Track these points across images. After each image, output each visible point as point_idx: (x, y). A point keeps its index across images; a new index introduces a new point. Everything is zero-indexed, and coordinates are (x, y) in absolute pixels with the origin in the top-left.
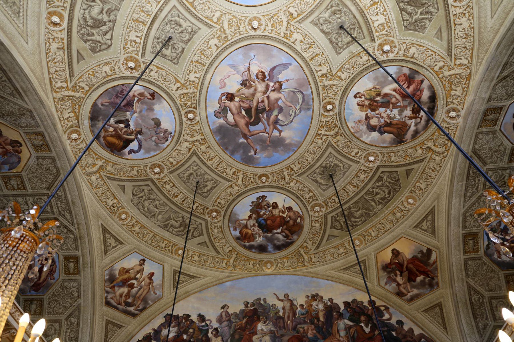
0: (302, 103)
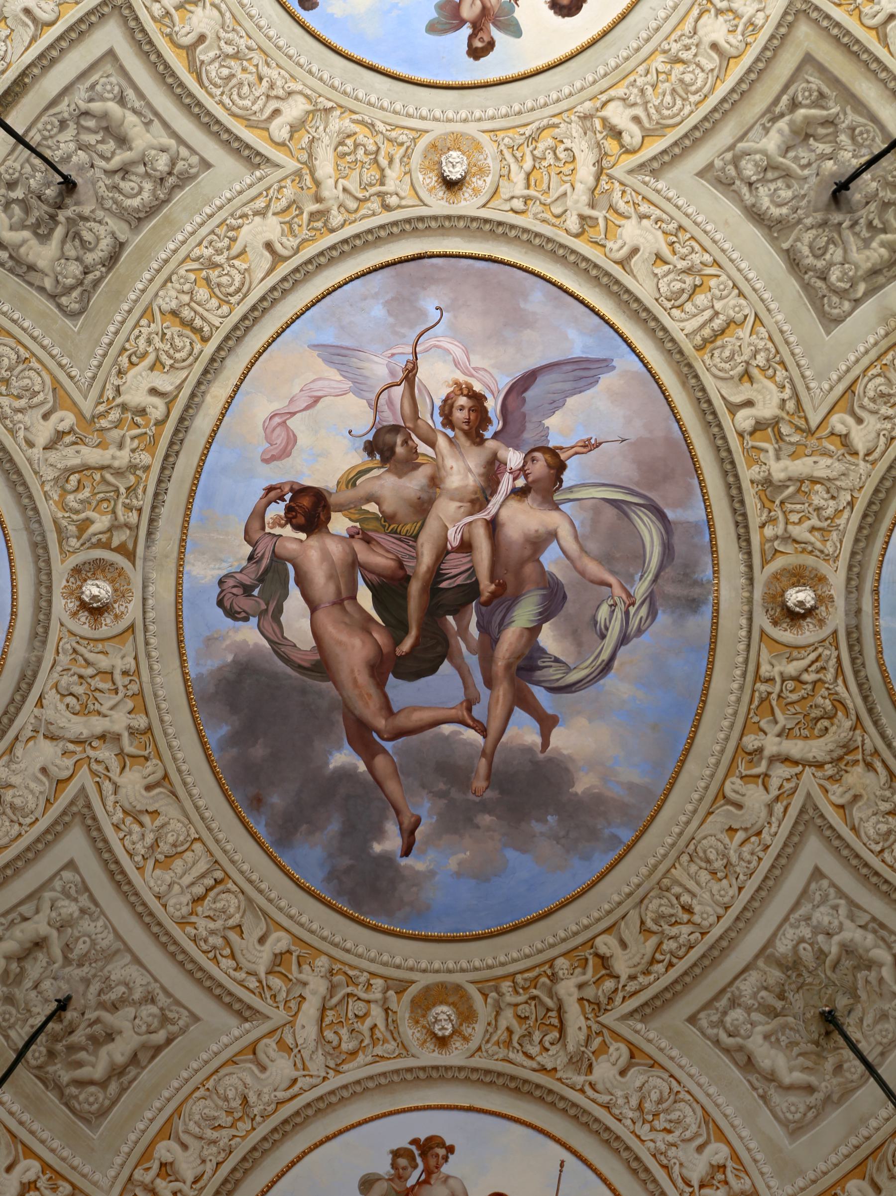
0: (661, 567)
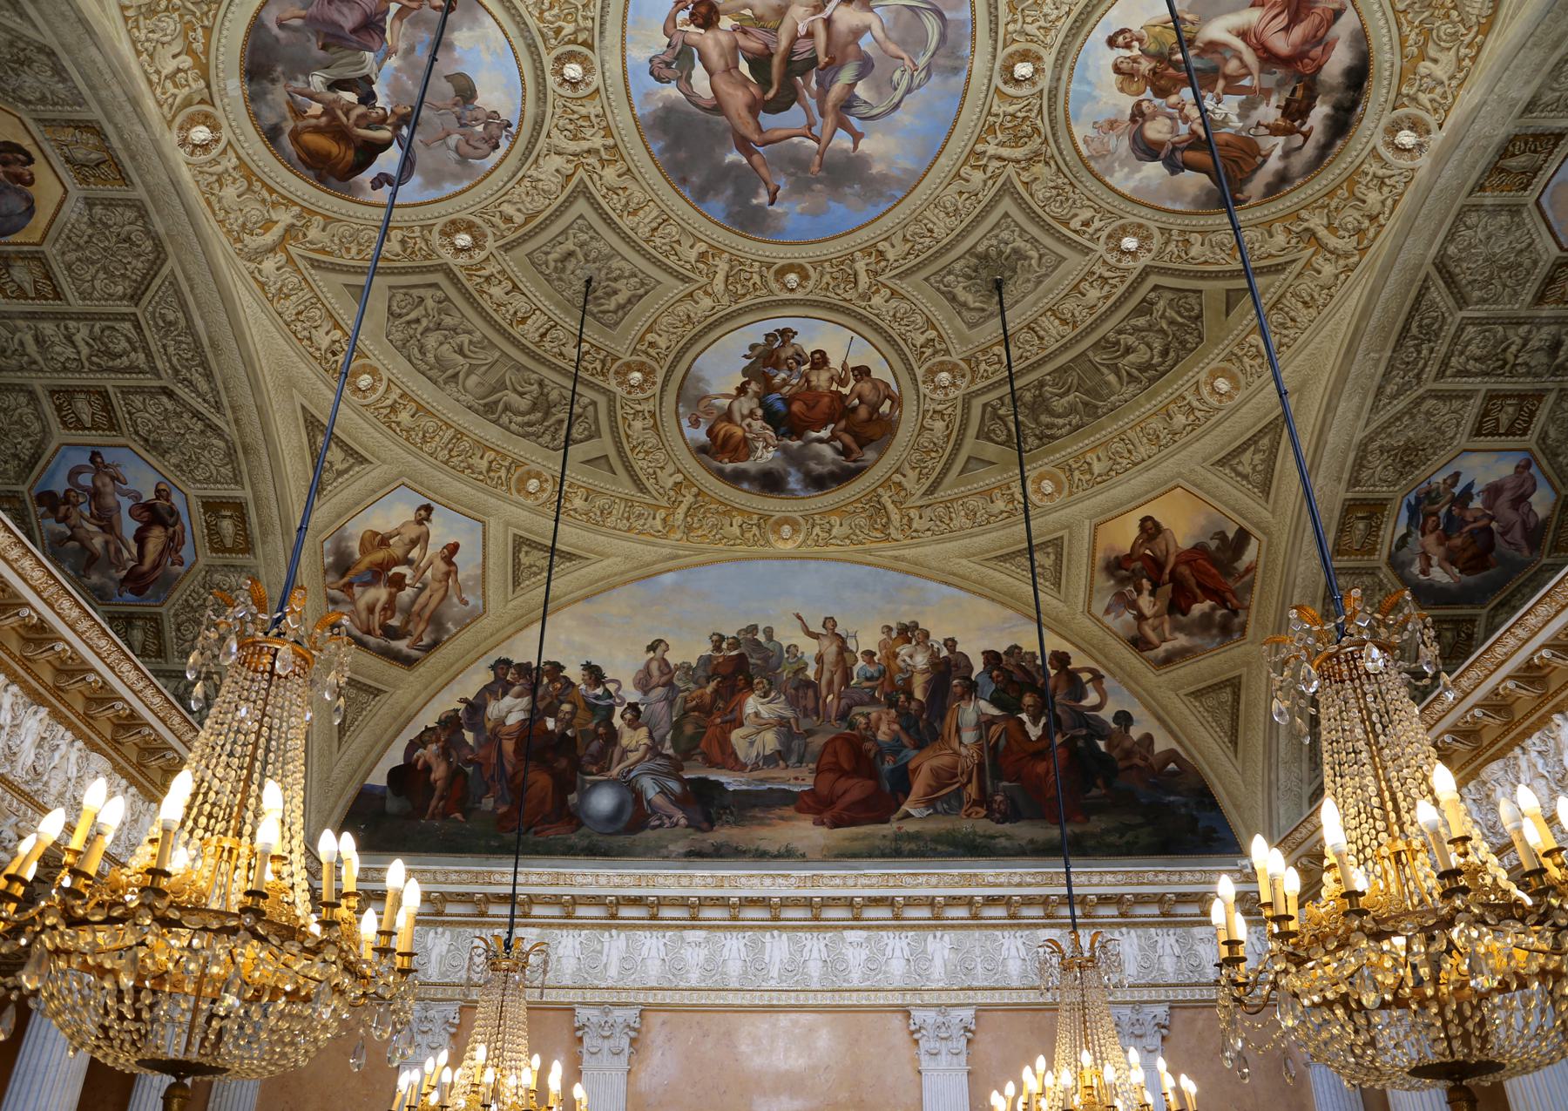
0: (937, 49)
